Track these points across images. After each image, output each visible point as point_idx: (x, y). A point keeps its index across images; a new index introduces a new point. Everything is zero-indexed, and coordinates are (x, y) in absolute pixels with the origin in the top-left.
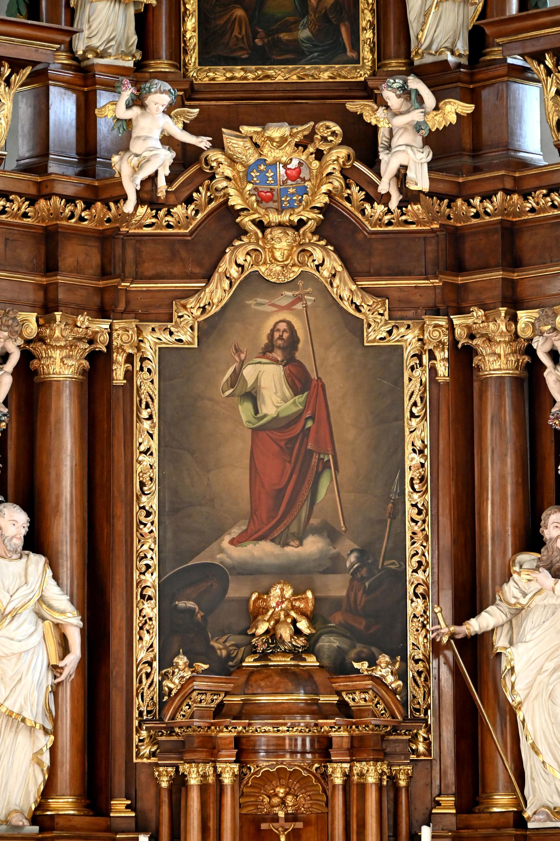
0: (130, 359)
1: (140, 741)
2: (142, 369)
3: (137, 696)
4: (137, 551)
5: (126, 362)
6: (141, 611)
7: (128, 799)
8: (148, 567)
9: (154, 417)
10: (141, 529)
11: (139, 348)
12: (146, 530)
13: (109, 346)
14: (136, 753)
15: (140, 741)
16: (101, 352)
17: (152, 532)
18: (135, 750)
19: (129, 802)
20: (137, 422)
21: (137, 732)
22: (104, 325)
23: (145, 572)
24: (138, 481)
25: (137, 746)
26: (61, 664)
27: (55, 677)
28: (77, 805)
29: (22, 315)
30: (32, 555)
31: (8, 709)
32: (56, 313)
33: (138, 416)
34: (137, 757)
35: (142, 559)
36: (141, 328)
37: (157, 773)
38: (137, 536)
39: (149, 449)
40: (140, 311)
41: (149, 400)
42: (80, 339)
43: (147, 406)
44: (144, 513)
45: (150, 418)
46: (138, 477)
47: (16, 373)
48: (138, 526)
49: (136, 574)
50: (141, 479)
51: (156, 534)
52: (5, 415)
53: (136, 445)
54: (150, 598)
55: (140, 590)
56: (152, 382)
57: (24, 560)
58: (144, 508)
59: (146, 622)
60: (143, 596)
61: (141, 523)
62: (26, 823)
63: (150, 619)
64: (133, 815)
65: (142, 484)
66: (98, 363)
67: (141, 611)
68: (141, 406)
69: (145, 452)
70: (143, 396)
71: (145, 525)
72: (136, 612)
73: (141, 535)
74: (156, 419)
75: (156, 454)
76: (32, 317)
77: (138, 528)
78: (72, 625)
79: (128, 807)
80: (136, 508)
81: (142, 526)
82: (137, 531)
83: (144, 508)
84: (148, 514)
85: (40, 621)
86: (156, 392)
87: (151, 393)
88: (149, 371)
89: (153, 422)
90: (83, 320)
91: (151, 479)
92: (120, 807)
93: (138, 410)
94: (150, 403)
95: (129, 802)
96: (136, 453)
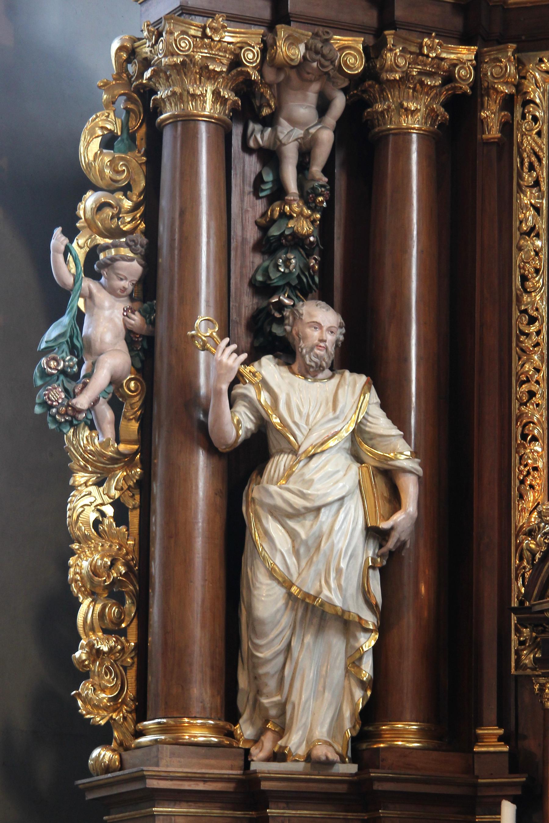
0: (508, 103)
1: (521, 643)
2: (524, 117)
3: (517, 580)
4: (517, 373)
5: (502, 109)
6: (521, 458)
7: (500, 727)
8: (532, 394)
9: (542, 184)
10: (522, 342)
11: (518, 86)
12: (528, 344)
13: (476, 85)
14: (516, 660)
15: (521, 643)
16: (465, 93)
17: (537, 344)
18: (513, 657)
19: (501, 732)
20: (518, 192)
21: (517, 631)
22: (466, 53)
23: (527, 401)
24: (518, 273)
25: (517, 653)
26: (385, 525)
27: (381, 546)
28: (421, 733)
29: (339, 40)
30: (347, 373)
31: (301, 590)
32: (386, 32)
33: (519, 185)
34: (516, 668)
35: (524, 382)
36: (524, 60)
37: (537, 687)
38: (517, 353)
39: (533, 228)
40: (523, 38)
41: (533, 159)
42: (430, 75)
43: (532, 167)
44: (525, 319)
45: (537, 183)
46: (518, 269)
47: (340, 129)
48: (518, 338)
49: (515, 405)
50: (522, 271)
51: (544, 345)
52: (322, 186)
53: (516, 224)
54: (535, 439)
55: (520, 429)
56: (539, 134)
57: (335, 381)
58: (525, 311)
59: (528, 473)
60: (524, 436)
61: (523, 333)
62: (336, 758)
63: (536, 469)
64: (506, 749)
65: (524, 279)
66: (460, 109)
67: (521, 458)
68: (522, 169)
69: (528, 234)
70: (525, 155)
71: (528, 335)
72: (515, 458)
73: (522, 350)
74: (544, 187)
75: (544, 236)
76: (357, 42)
77: (518, 338)
78: (405, 471)
79: (501, 738)
80: (516, 314)
81: (522, 338)
82: (517, 345)
83: (525, 311)
84: (532, 320)
85: (355, 467)
86: (544, 147)
87: (537, 149)
88: (535, 119)
89: (540, 190)
90: (435, 49)
91: (537, 271)
92: (491, 741)
93: (520, 177)
94: (536, 164)
95: (501, 732)
96: (516, 234)
